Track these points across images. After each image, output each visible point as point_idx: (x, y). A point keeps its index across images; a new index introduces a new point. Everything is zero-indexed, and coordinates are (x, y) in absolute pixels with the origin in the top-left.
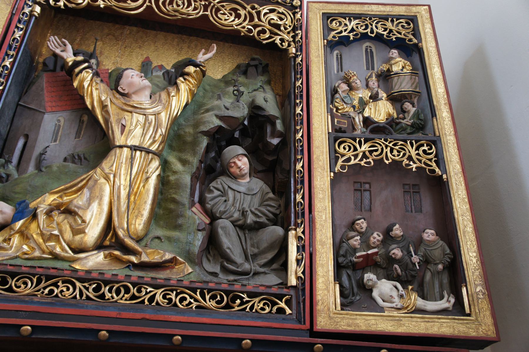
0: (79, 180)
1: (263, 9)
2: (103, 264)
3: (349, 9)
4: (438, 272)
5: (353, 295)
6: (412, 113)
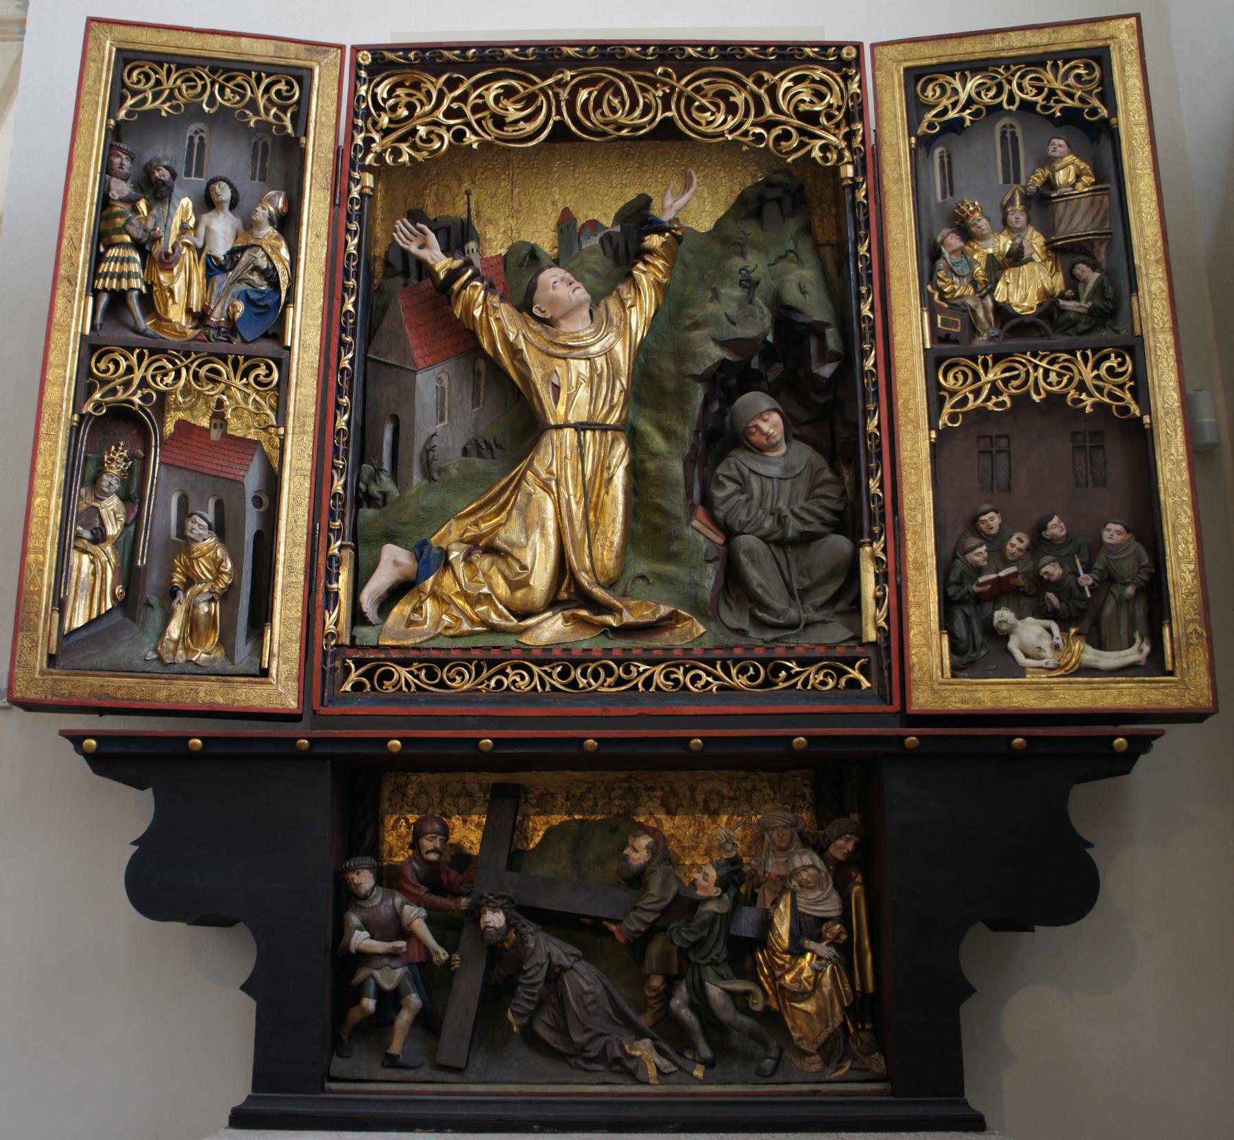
0: (497, 488)
1: (782, 79)
2: (564, 633)
3: (962, 50)
5: (975, 649)
6: (1090, 285)
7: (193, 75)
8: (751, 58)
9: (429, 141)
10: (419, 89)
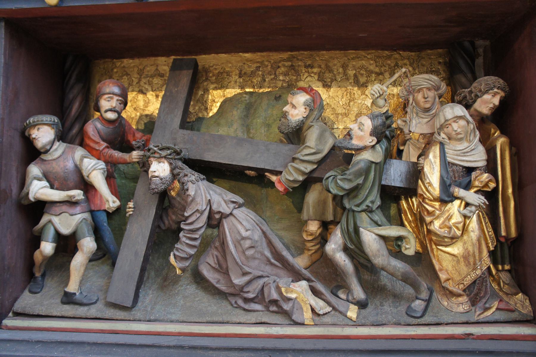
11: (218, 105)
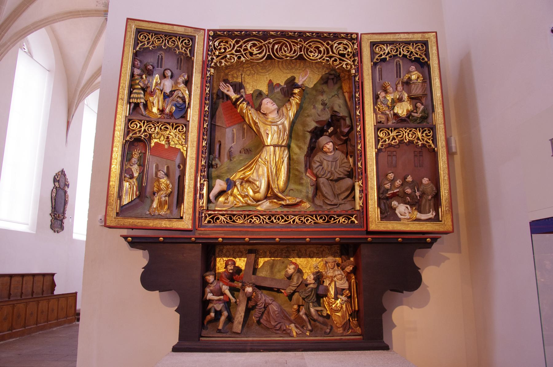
1: (335, 43)
2: (269, 206)
3: (387, 38)
4: (429, 200)
7: (159, 37)
8: (326, 37)
9: (231, 59)
10: (228, 43)
11: (262, 263)
